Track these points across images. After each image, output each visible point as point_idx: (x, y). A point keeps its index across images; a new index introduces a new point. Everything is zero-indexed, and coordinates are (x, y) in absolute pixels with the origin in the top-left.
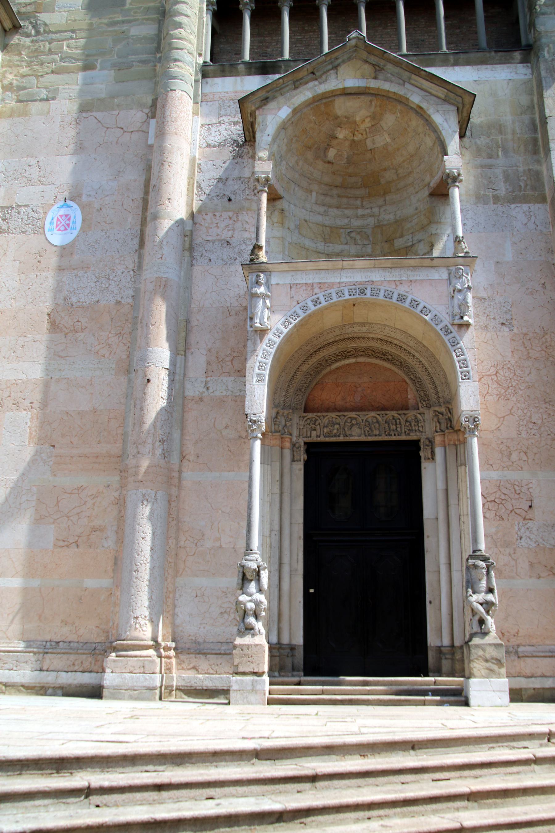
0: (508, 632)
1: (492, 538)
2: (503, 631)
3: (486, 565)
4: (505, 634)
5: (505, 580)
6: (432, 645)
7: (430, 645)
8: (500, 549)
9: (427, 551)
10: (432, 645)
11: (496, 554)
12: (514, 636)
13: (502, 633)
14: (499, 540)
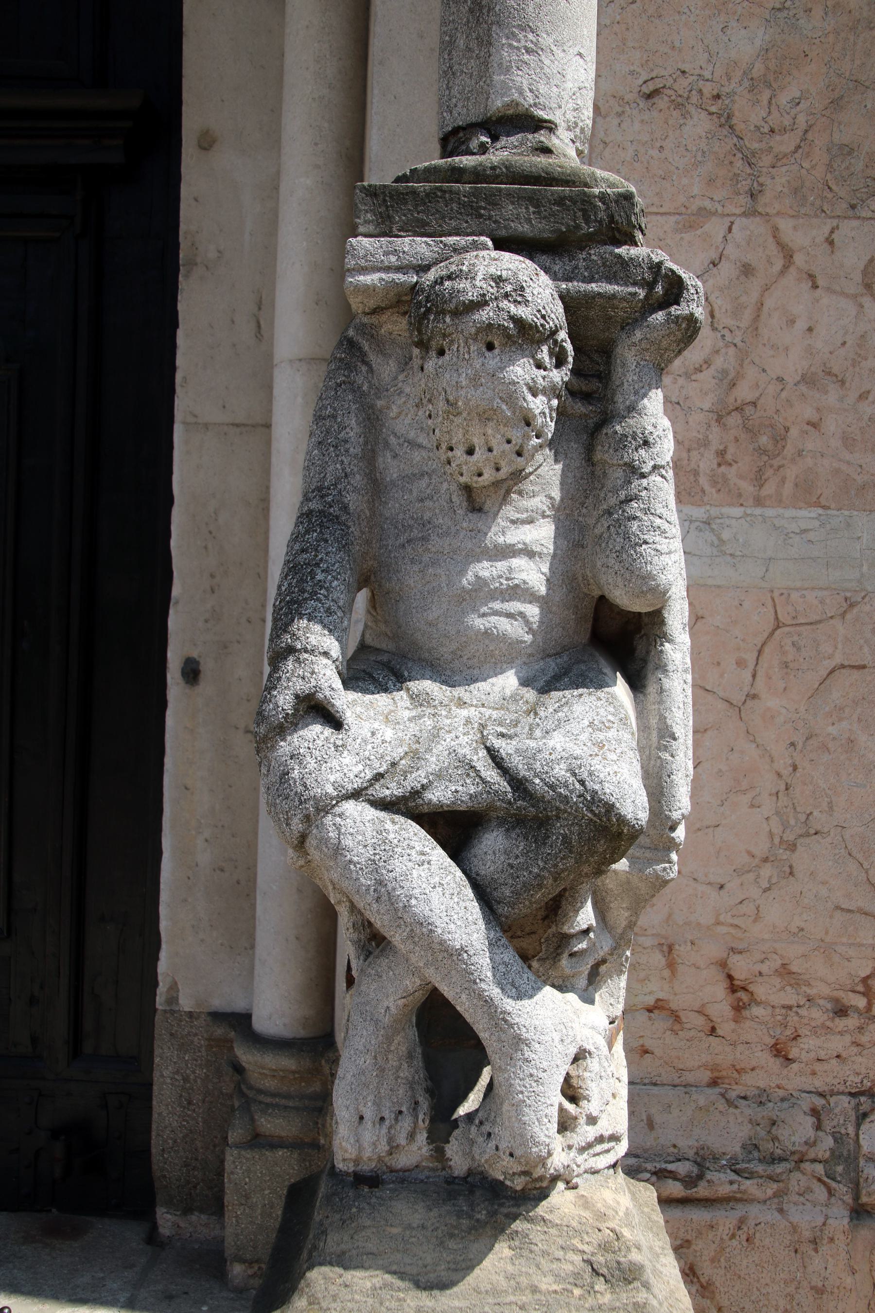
0: (785, 971)
1: (726, 120)
2: (741, 968)
3: (564, 297)
4: (760, 990)
5: (807, 516)
6: (186, 1004)
7: (172, 1000)
8: (785, 225)
9: (192, 263)
10: (186, 1004)
11: (747, 270)
12: (841, 1011)
13: (733, 986)
14: (785, 143)
